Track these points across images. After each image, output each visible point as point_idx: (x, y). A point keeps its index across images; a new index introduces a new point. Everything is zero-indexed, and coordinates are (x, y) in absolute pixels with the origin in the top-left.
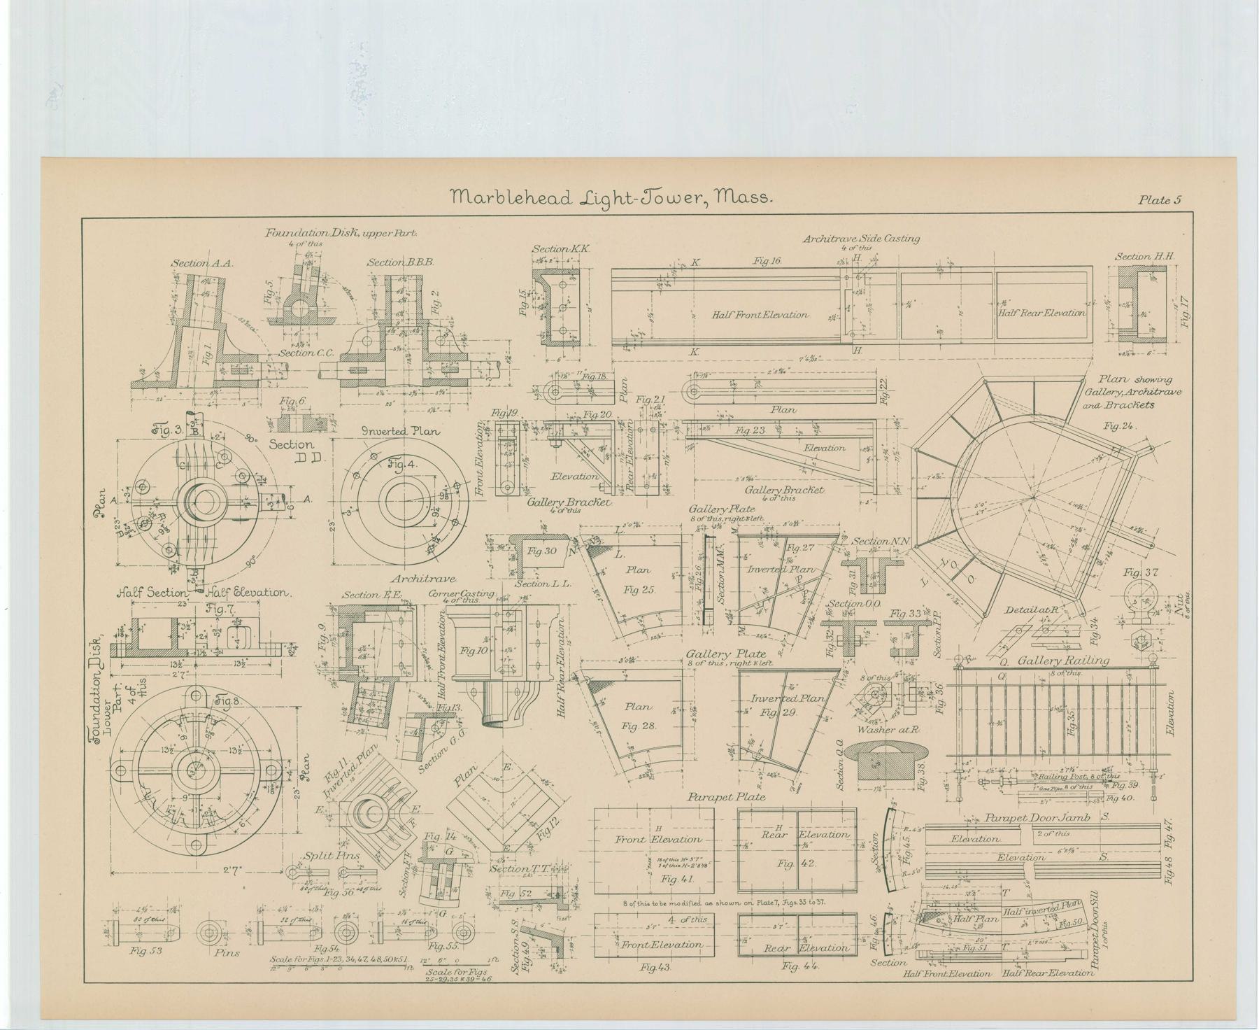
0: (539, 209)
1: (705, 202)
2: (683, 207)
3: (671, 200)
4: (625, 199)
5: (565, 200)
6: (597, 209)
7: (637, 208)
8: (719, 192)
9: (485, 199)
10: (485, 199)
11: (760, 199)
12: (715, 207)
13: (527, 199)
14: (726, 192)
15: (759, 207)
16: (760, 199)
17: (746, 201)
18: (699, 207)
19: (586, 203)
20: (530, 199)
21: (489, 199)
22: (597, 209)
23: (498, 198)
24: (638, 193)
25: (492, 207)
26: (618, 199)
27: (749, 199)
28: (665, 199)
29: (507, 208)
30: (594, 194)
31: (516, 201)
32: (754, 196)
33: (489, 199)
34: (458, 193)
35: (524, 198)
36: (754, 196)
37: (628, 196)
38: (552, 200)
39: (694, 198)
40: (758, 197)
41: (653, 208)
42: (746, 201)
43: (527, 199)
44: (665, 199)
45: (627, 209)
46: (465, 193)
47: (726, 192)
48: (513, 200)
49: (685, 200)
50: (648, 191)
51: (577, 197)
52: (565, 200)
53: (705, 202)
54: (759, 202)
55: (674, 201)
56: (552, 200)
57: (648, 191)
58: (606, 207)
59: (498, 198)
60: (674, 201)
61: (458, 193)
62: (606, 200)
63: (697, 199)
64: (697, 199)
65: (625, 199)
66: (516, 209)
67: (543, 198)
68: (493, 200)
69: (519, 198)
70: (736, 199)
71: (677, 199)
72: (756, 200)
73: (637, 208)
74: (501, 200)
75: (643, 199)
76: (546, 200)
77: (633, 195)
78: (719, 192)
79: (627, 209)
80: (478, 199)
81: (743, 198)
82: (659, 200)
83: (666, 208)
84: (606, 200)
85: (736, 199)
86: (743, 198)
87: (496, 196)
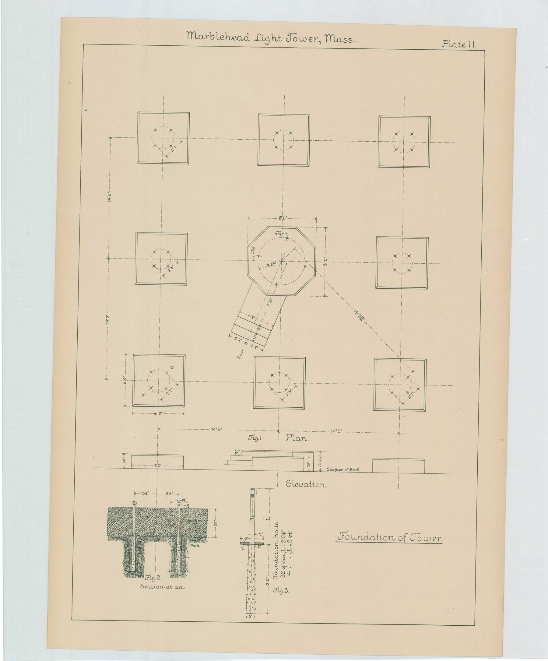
0: (232, 43)
1: (319, 42)
2: (307, 44)
3: (302, 40)
4: (277, 39)
5: (246, 39)
6: (262, 44)
7: (284, 43)
8: (327, 36)
9: (204, 37)
10: (204, 37)
12: (325, 44)
13: (226, 37)
14: (330, 36)
15: (348, 45)
16: (348, 40)
17: (341, 41)
18: (316, 44)
19: (257, 40)
20: (228, 37)
21: (206, 37)
25: (208, 41)
27: (343, 40)
28: (298, 39)
29: (215, 42)
30: (261, 36)
31: (221, 38)
32: (345, 39)
33: (206, 37)
34: (190, 33)
35: (225, 37)
36: (345, 39)
37: (279, 37)
38: (239, 38)
40: (348, 39)
41: (292, 44)
42: (341, 41)
43: (226, 37)
44: (298, 39)
46: (194, 33)
47: (330, 36)
48: (219, 38)
49: (309, 40)
50: (290, 35)
51: (253, 37)
52: (246, 39)
53: (319, 42)
54: (348, 42)
55: (303, 40)
56: (239, 38)
58: (267, 43)
59: (211, 36)
60: (303, 40)
61: (190, 33)
62: (267, 39)
63: (315, 39)
64: (315, 39)
65: (277, 39)
66: (221, 42)
68: (209, 38)
69: (222, 37)
71: (305, 40)
73: (284, 43)
74: (212, 37)
75: (287, 39)
76: (236, 38)
77: (282, 37)
78: (327, 36)
79: (278, 44)
82: (295, 39)
83: (299, 44)
84: (267, 39)
86: (339, 40)
87: (210, 36)
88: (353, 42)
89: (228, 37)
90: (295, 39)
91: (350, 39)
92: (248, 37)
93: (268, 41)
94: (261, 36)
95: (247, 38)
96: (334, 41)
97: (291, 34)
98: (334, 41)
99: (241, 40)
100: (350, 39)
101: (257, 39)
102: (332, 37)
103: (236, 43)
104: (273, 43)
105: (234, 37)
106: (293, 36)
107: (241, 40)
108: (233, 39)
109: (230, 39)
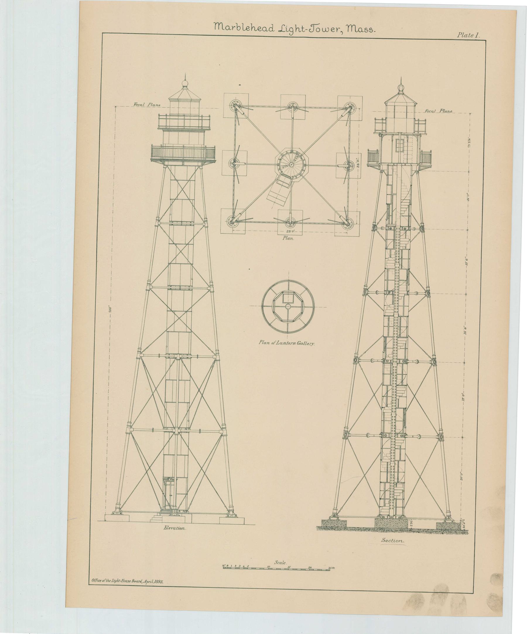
0: (257, 33)
1: (341, 32)
2: (330, 34)
3: (324, 30)
5: (271, 29)
6: (287, 34)
8: (348, 27)
9: (231, 28)
10: (231, 28)
11: (369, 30)
13: (252, 28)
14: (352, 27)
15: (369, 35)
16: (369, 30)
17: (362, 31)
19: (281, 31)
20: (253, 28)
21: (233, 28)
22: (287, 34)
23: (237, 27)
24: (307, 26)
25: (235, 32)
26: (298, 29)
30: (285, 27)
31: (246, 29)
32: (366, 29)
33: (233, 28)
35: (250, 28)
36: (366, 29)
37: (302, 28)
39: (336, 29)
40: (368, 29)
41: (315, 34)
42: (362, 31)
43: (252, 28)
45: (302, 34)
46: (221, 25)
47: (352, 27)
48: (245, 29)
49: (331, 30)
50: (313, 25)
51: (277, 28)
52: (271, 29)
53: (341, 32)
55: (326, 31)
56: (264, 29)
57: (313, 25)
58: (291, 33)
59: (237, 27)
60: (326, 31)
62: (291, 30)
63: (337, 30)
64: (337, 30)
65: (301, 29)
67: (260, 28)
68: (235, 29)
69: (248, 28)
70: (357, 30)
72: (366, 31)
74: (239, 28)
75: (310, 29)
76: (261, 29)
78: (348, 27)
79: (302, 34)
80: (227, 28)
81: (360, 30)
82: (318, 30)
83: (321, 34)
84: (291, 30)
85: (357, 30)
86: (360, 30)
88: (374, 31)
89: (254, 28)
90: (318, 30)
91: (371, 29)
92: (272, 28)
93: (291, 30)
94: (285, 27)
95: (272, 29)
96: (355, 31)
97: (314, 24)
98: (355, 31)
99: (266, 30)
100: (371, 29)
101: (281, 30)
102: (354, 27)
103: (261, 33)
104: (296, 34)
105: (259, 28)
106: (316, 27)
107: (266, 30)
108: (258, 29)
109: (256, 30)
